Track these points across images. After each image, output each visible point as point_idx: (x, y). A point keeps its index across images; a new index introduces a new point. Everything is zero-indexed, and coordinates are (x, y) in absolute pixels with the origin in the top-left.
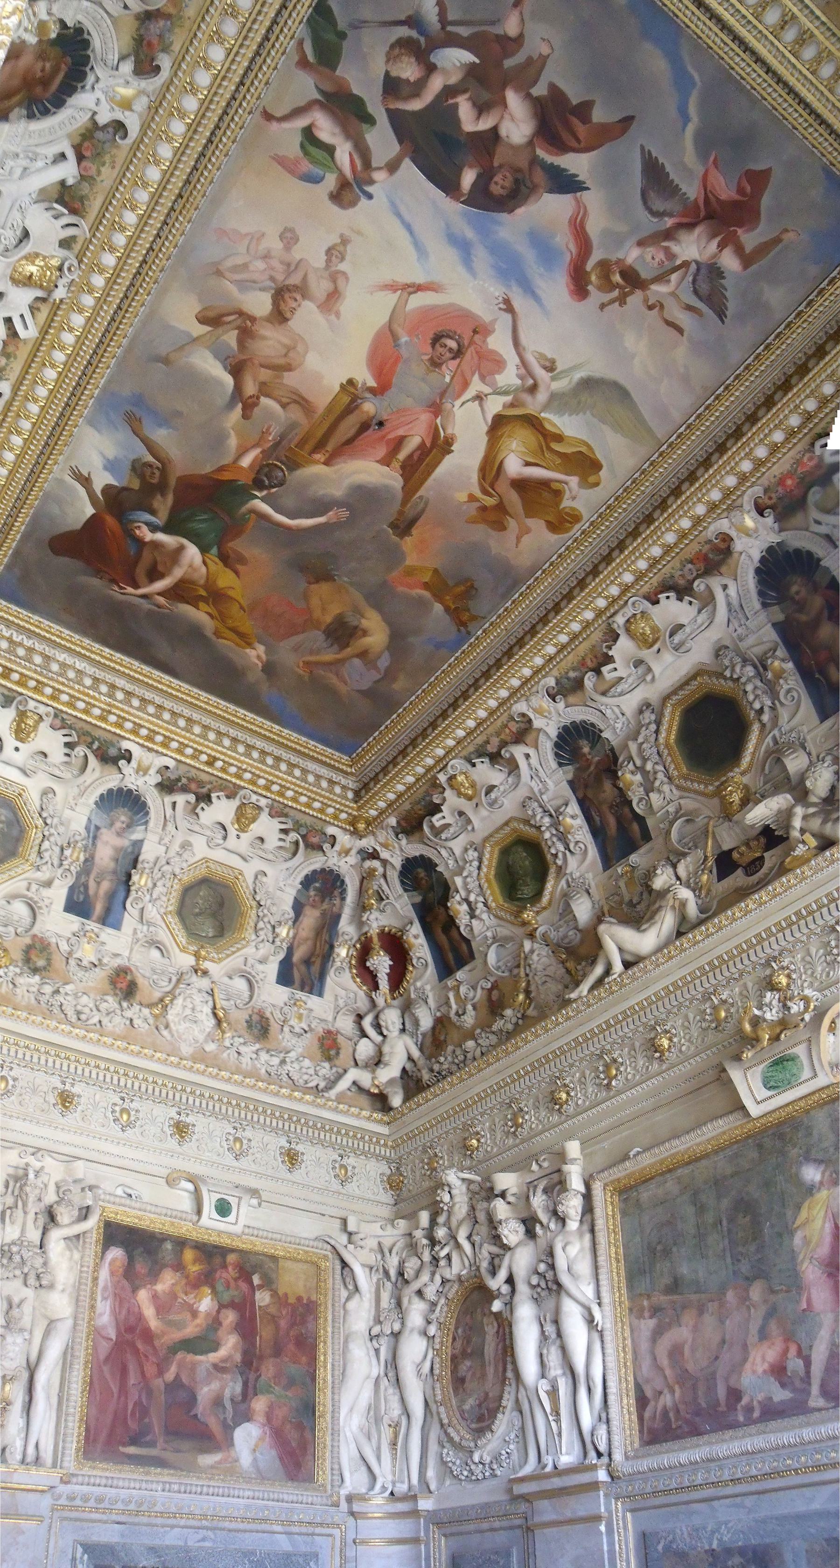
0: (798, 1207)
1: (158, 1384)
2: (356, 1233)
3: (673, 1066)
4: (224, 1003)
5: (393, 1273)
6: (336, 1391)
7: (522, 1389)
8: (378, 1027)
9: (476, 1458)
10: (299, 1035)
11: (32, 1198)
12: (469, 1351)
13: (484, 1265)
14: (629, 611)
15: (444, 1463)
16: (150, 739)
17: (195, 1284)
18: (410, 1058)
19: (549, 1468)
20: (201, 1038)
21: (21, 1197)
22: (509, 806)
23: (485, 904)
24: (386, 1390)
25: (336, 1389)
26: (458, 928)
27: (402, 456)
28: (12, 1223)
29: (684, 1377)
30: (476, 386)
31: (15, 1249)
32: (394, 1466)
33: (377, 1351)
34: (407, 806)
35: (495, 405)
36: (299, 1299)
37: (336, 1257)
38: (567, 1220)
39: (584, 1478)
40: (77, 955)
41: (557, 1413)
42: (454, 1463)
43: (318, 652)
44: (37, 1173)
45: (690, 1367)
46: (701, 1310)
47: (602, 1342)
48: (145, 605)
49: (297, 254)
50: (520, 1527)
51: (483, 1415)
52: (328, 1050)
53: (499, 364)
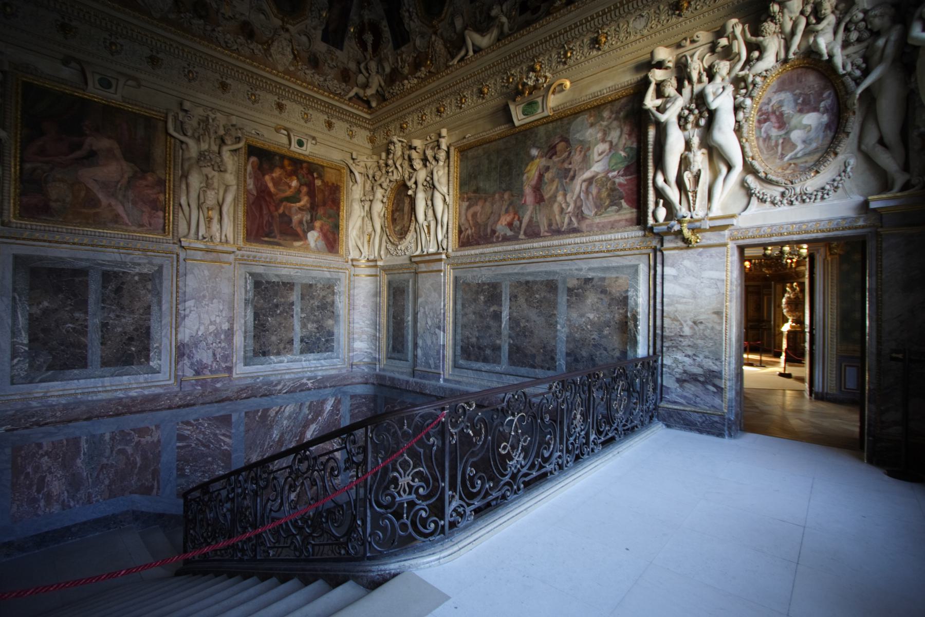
0: (527, 165)
1: (276, 214)
3: (487, 101)
4: (297, 47)
5: (370, 176)
8: (367, 69)
9: (399, 248)
10: (332, 68)
11: (212, 131)
13: (406, 176)
15: (387, 249)
17: (290, 175)
18: (380, 86)
20: (287, 64)
21: (206, 129)
23: (417, 14)
25: (347, 221)
26: (404, 25)
28: (204, 142)
29: (476, 224)
31: (206, 153)
33: (363, 206)
36: (333, 184)
39: (438, 257)
40: (222, 11)
41: (429, 232)
44: (213, 120)
45: (479, 221)
46: (485, 200)
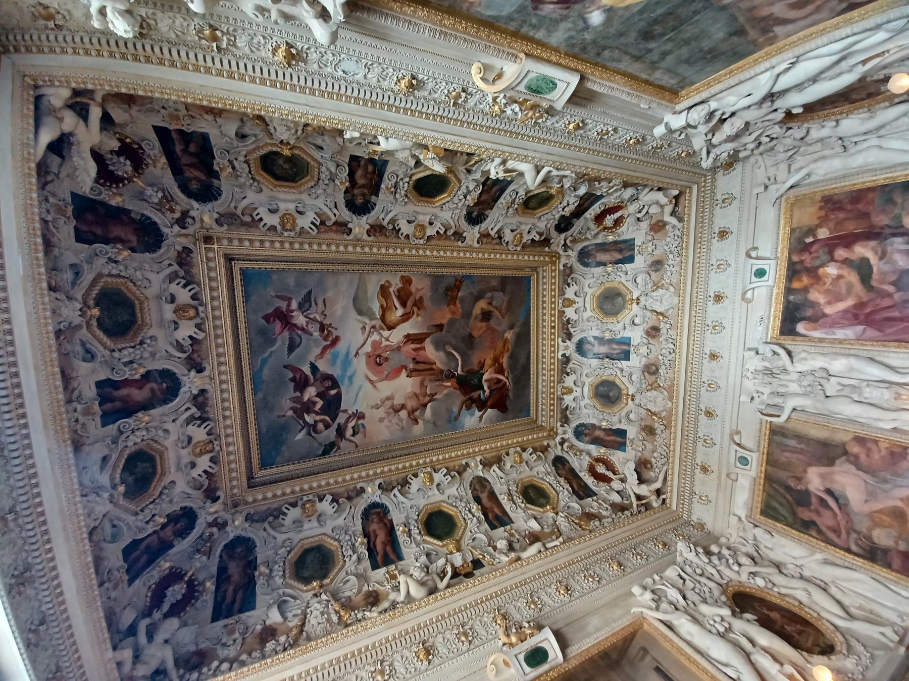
14: (417, 241)
16: (554, 352)
22: (515, 220)
27: (419, 346)
30: (385, 343)
34: (538, 249)
35: (386, 333)
43: (497, 318)
48: (510, 376)
49: (384, 415)
52: (660, 226)
53: (374, 343)
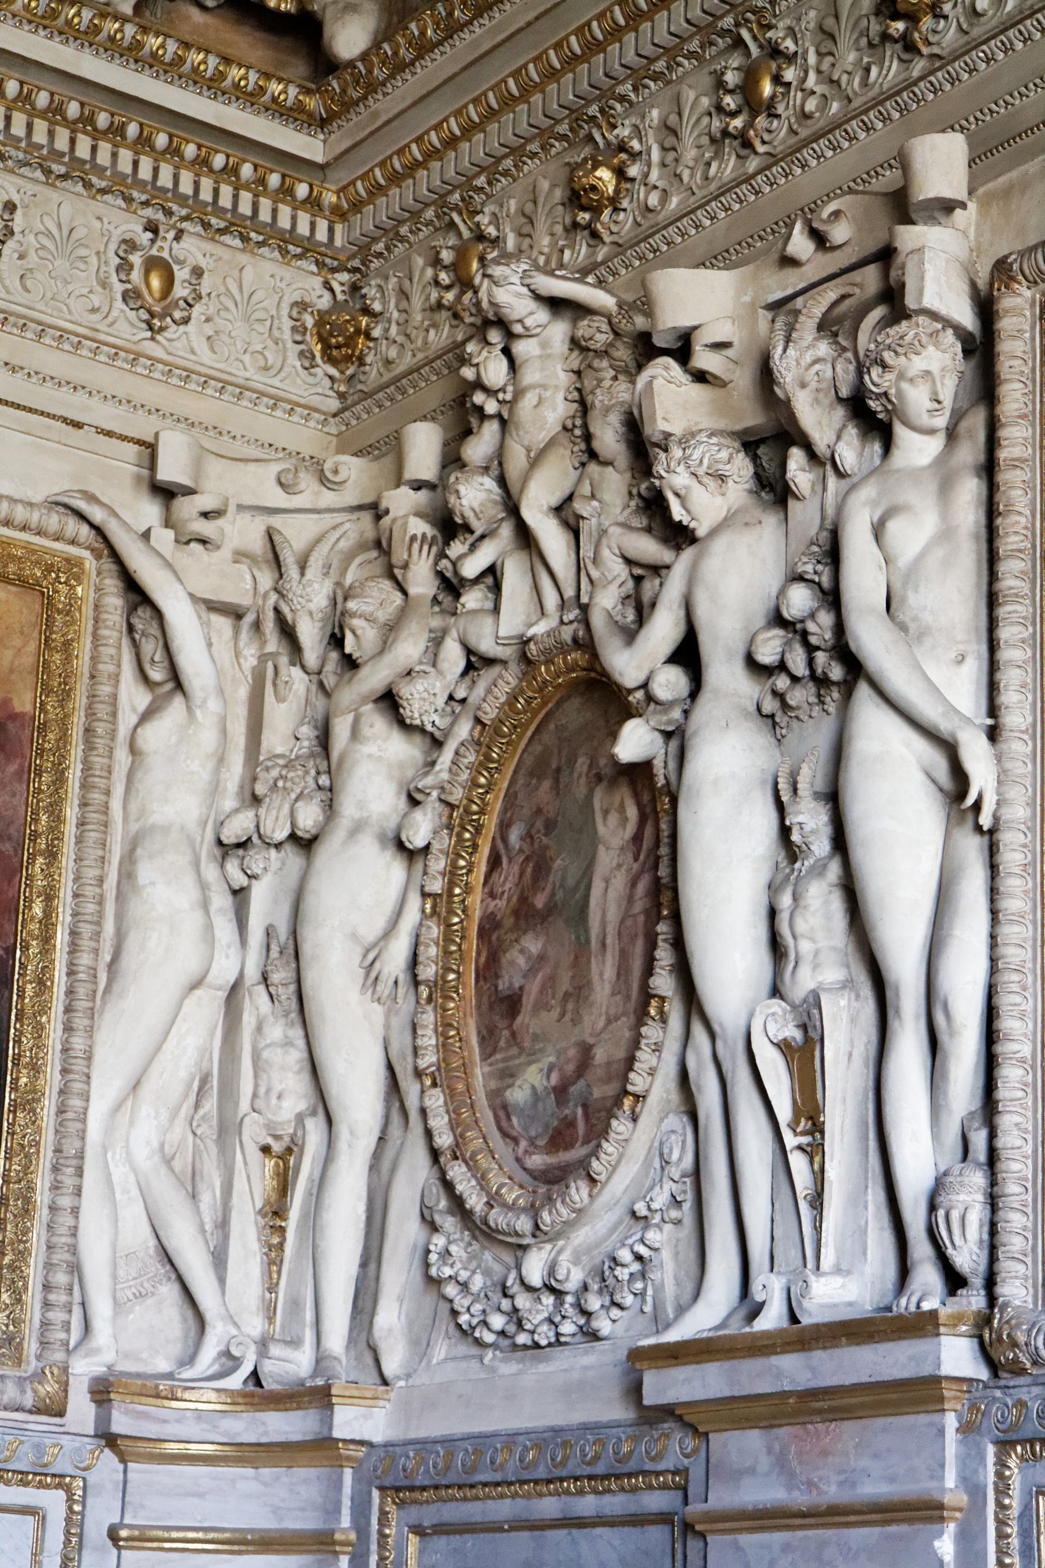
2: (190, 492)
6: (80, 1022)
7: (699, 1032)
9: (535, 1270)
12: (540, 901)
19: (772, 1319)
24: (259, 1029)
32: (272, 1288)
33: (240, 895)
37: (108, 565)
38: (900, 431)
42: (464, 1286)
47: (993, 869)
50: (664, 1518)
51: (571, 1124)
